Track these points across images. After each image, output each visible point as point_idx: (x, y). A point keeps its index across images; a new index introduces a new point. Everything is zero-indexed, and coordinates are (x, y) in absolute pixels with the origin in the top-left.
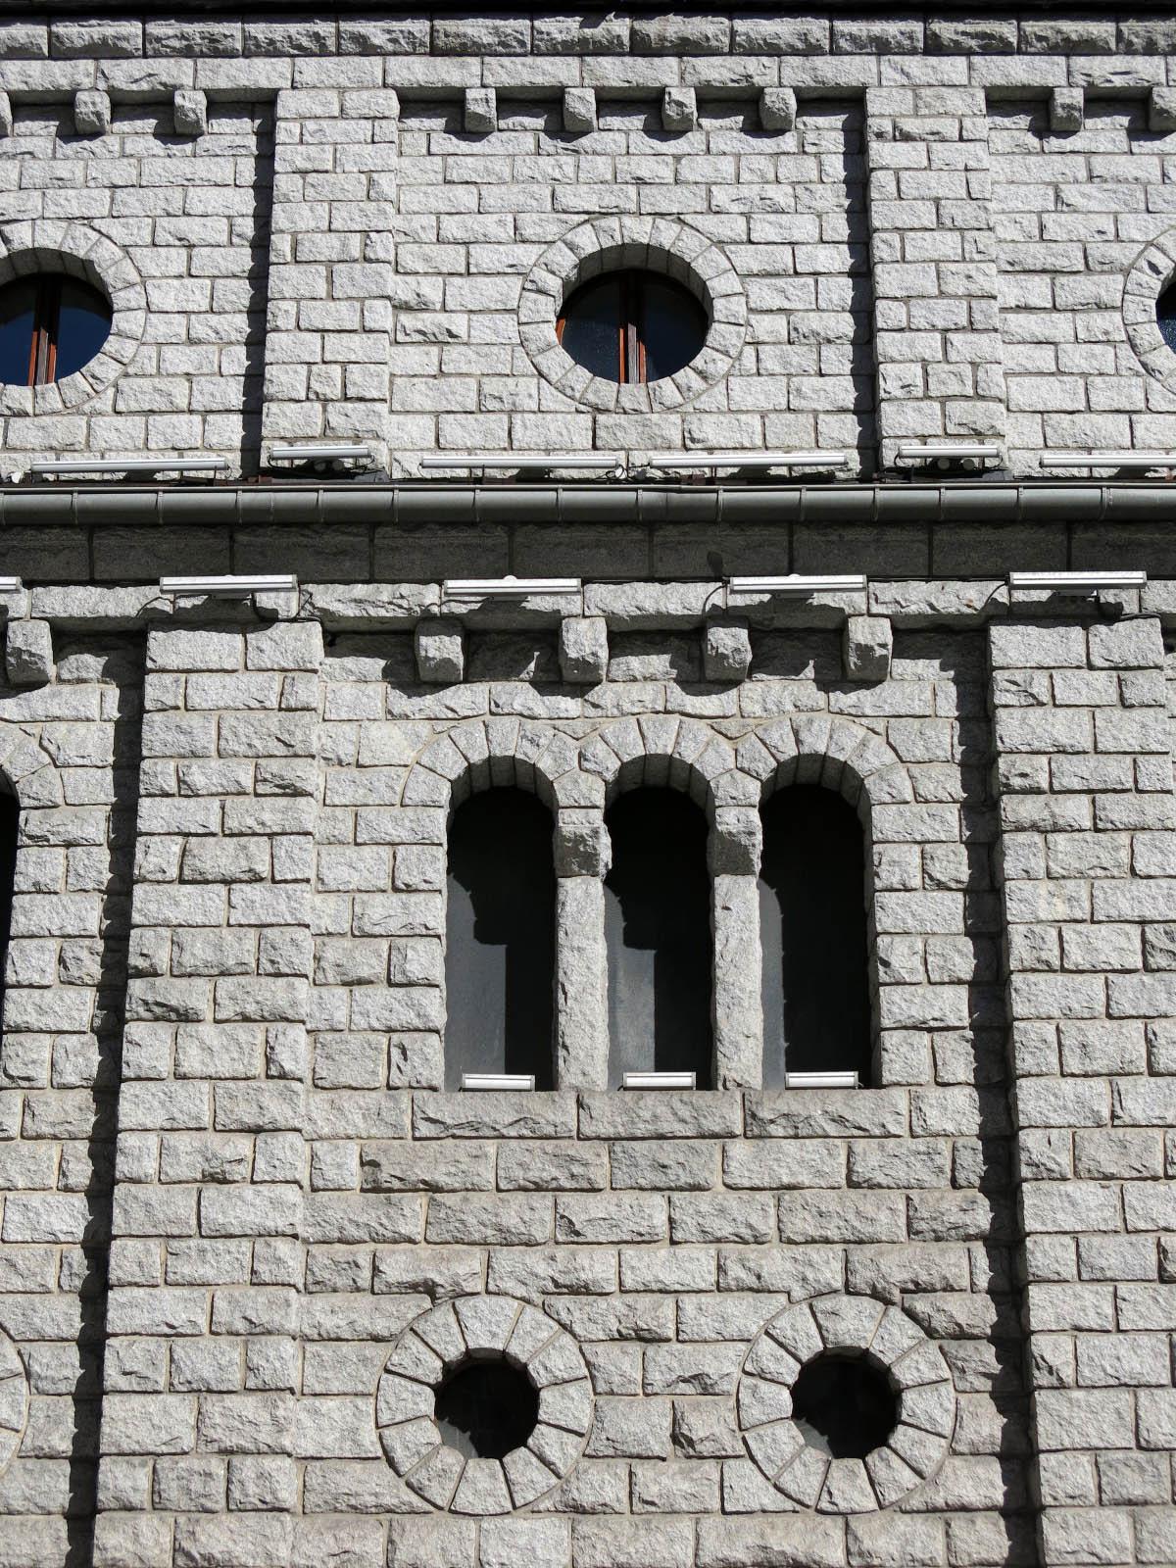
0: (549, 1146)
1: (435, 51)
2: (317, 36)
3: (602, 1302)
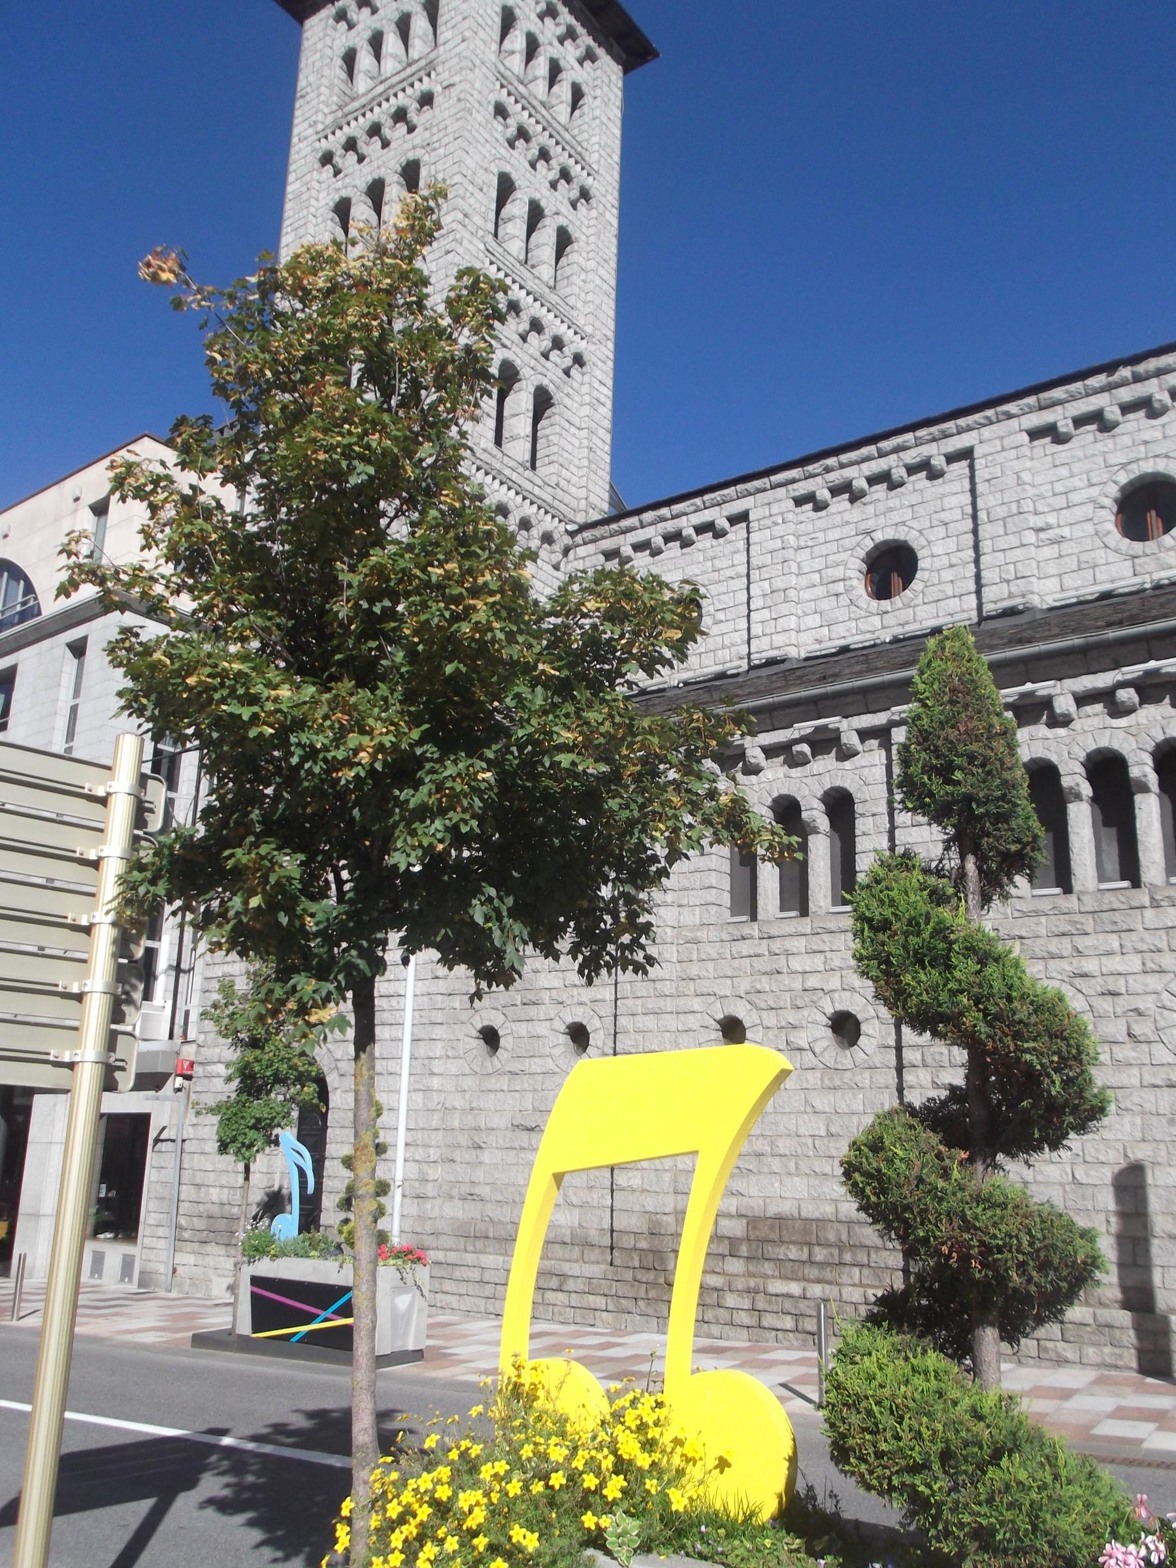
0: (1067, 917)
1: (1041, 408)
2: (987, 418)
3: (1093, 981)
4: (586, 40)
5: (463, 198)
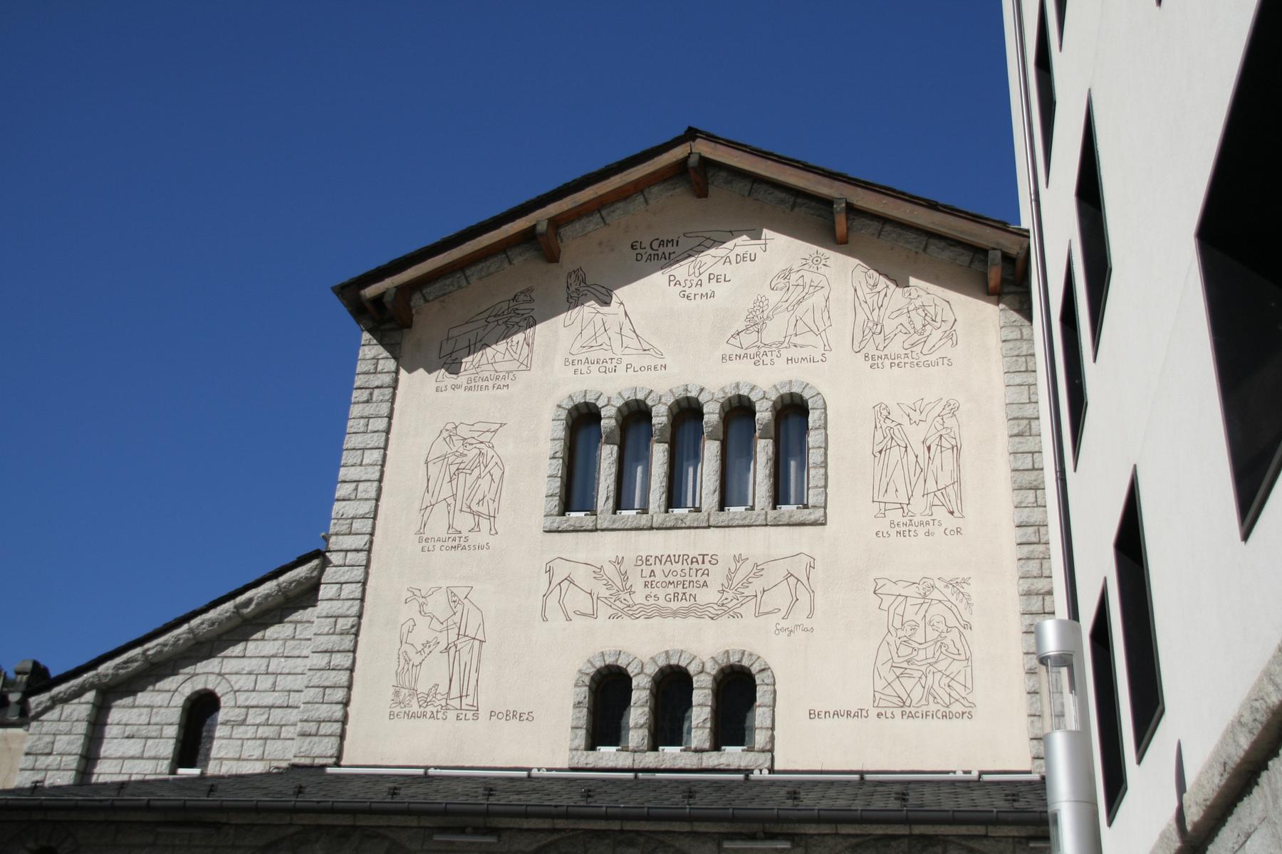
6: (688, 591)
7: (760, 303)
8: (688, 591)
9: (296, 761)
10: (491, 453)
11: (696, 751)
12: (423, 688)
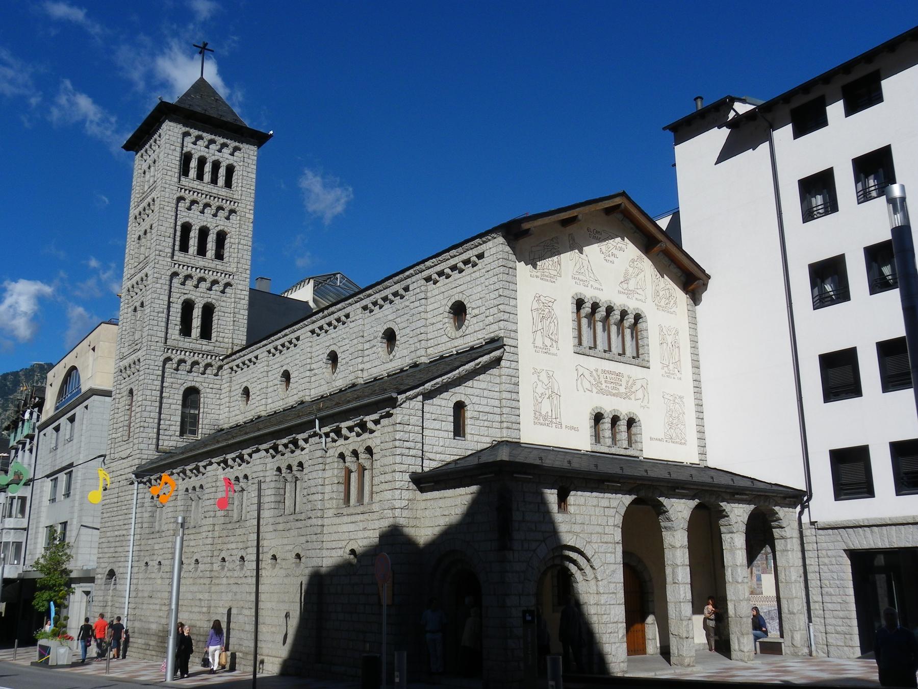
4: (233, 144)
5: (159, 245)
6: (618, 387)
7: (627, 270)
8: (618, 387)
9: (507, 439)
10: (553, 313)
11: (625, 448)
12: (544, 413)
